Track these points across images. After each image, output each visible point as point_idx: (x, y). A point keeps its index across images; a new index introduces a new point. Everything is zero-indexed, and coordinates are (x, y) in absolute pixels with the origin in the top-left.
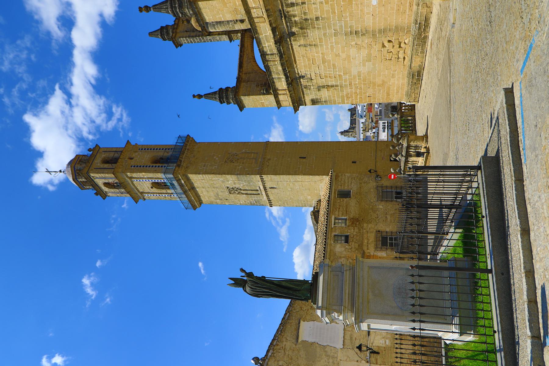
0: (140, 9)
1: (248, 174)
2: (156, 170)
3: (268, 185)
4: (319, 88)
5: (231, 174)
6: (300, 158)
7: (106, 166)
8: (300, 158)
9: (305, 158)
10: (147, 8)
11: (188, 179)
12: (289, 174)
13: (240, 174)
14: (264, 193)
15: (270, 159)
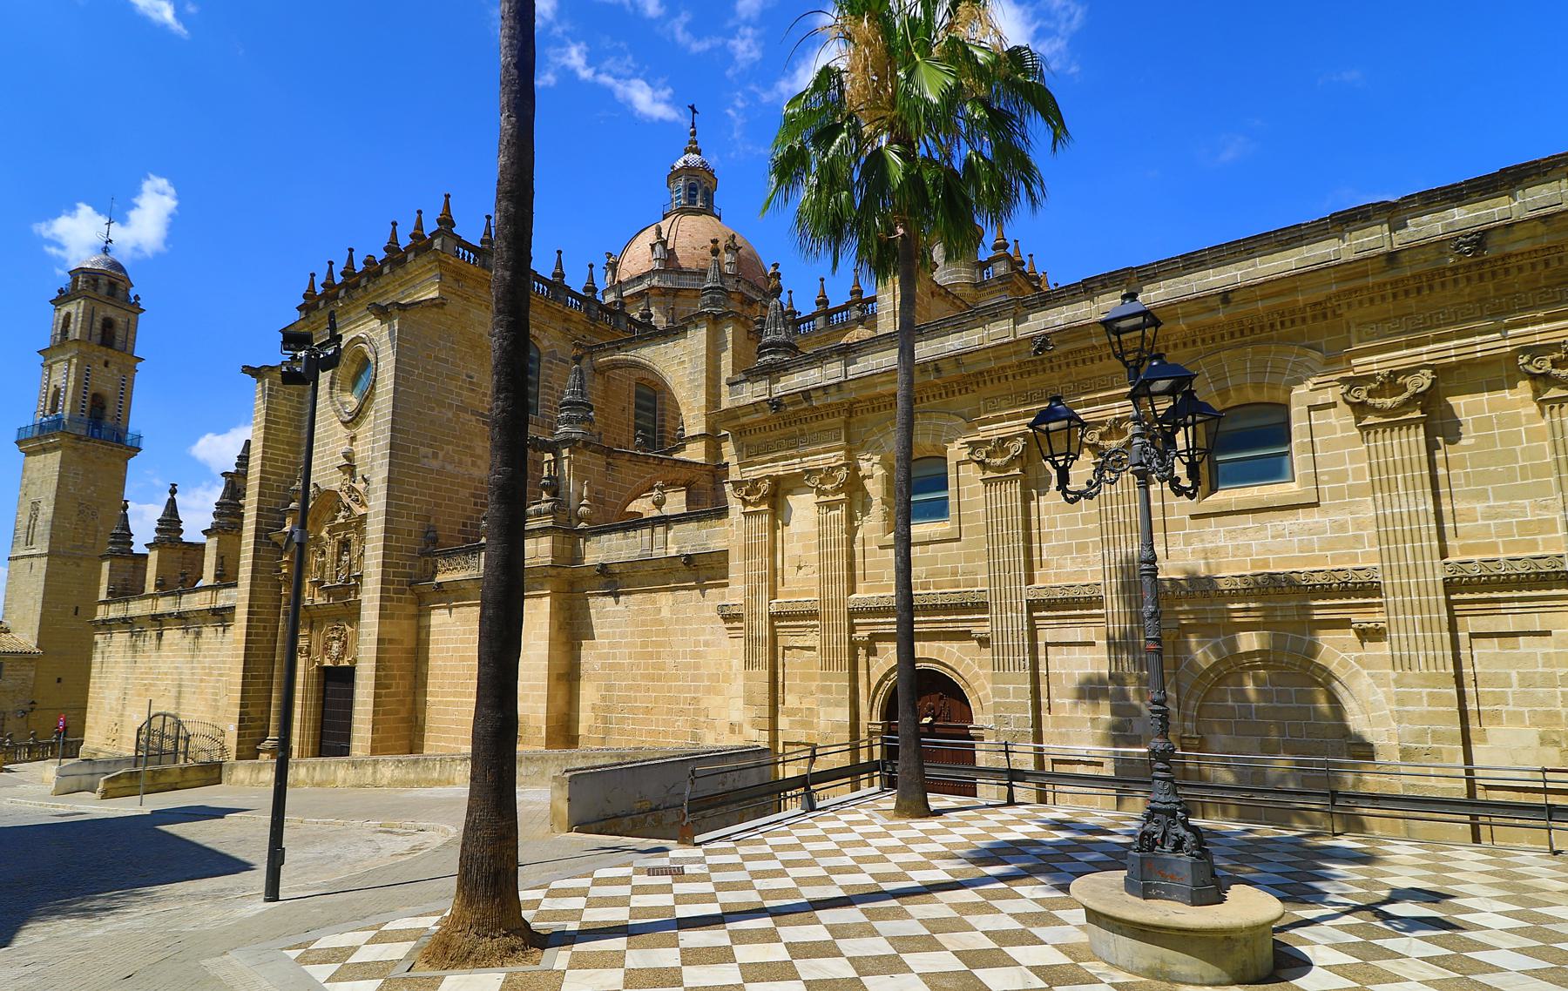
0: (174, 485)
1: (51, 537)
2: (76, 402)
3: (35, 560)
4: (103, 652)
5: (54, 513)
6: (77, 608)
7: (98, 325)
8: (77, 608)
9: (76, 614)
10: (173, 492)
11: (55, 448)
12: (45, 594)
13: (52, 525)
14: (27, 553)
15: (78, 566)
